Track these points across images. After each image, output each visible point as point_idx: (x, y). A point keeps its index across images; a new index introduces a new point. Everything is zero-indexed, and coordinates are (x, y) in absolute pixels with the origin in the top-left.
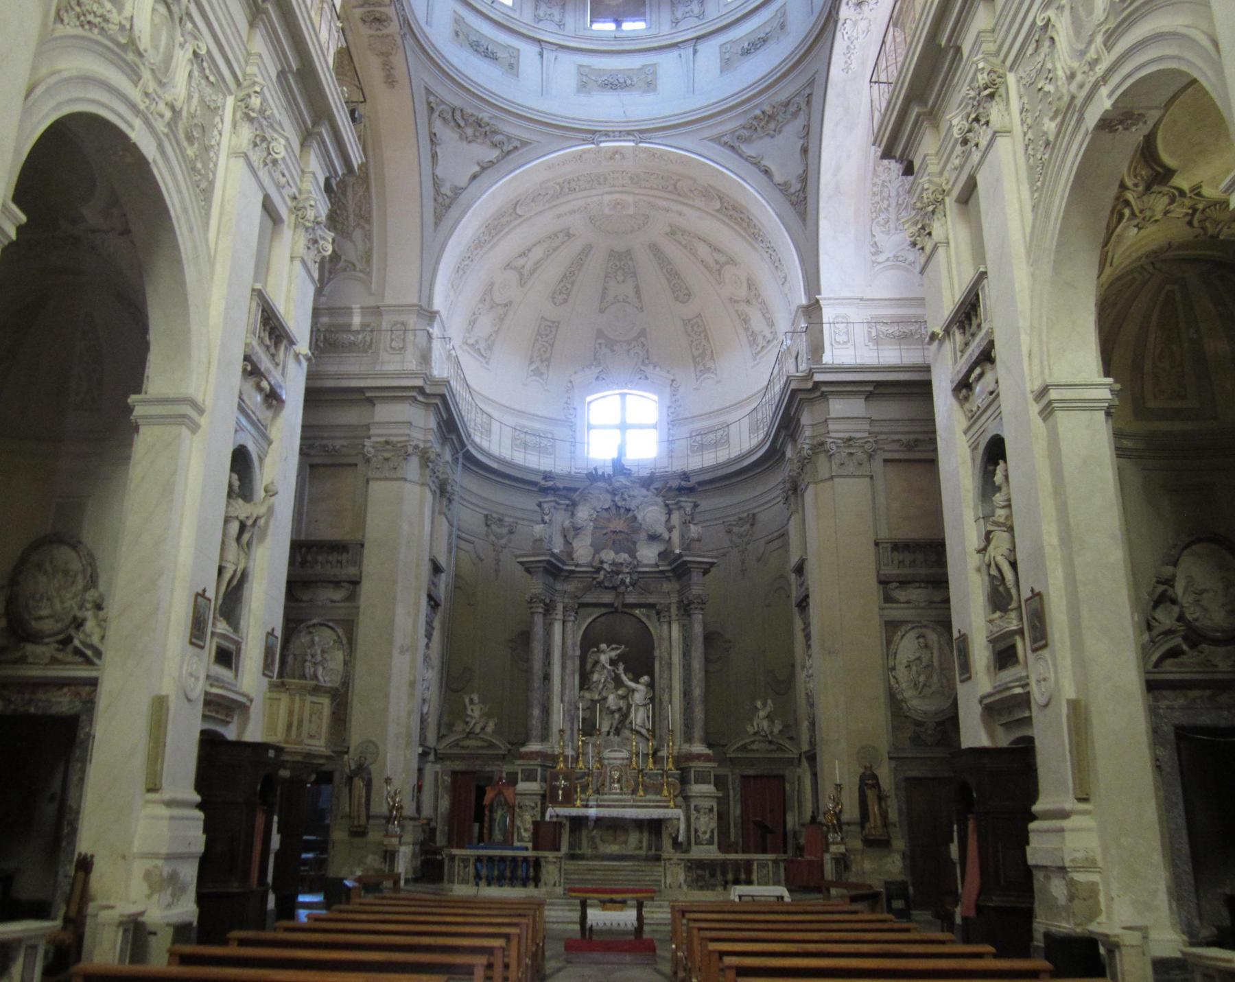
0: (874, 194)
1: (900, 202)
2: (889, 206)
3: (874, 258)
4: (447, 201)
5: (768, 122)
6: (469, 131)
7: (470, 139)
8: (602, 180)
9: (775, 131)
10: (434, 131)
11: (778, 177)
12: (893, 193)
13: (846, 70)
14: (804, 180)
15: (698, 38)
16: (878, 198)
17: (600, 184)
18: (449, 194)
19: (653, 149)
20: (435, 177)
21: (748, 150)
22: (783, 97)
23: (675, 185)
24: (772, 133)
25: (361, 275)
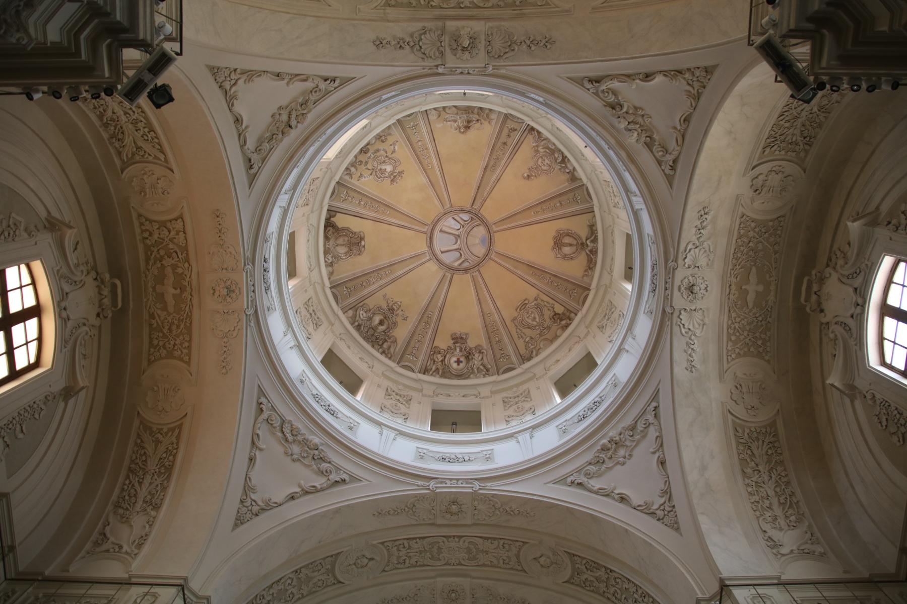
0: (750, 494)
1: (782, 501)
2: (770, 504)
3: (774, 551)
4: (255, 509)
5: (615, 450)
6: (296, 449)
7: (295, 457)
8: (435, 550)
9: (625, 457)
10: (258, 432)
11: (636, 500)
12: (771, 493)
13: (691, 368)
14: (667, 493)
15: (534, 427)
16: (756, 498)
17: (432, 558)
18: (260, 503)
19: (493, 495)
20: (247, 478)
21: (596, 484)
22: (628, 421)
23: (518, 556)
24: (621, 459)
25: (126, 556)
